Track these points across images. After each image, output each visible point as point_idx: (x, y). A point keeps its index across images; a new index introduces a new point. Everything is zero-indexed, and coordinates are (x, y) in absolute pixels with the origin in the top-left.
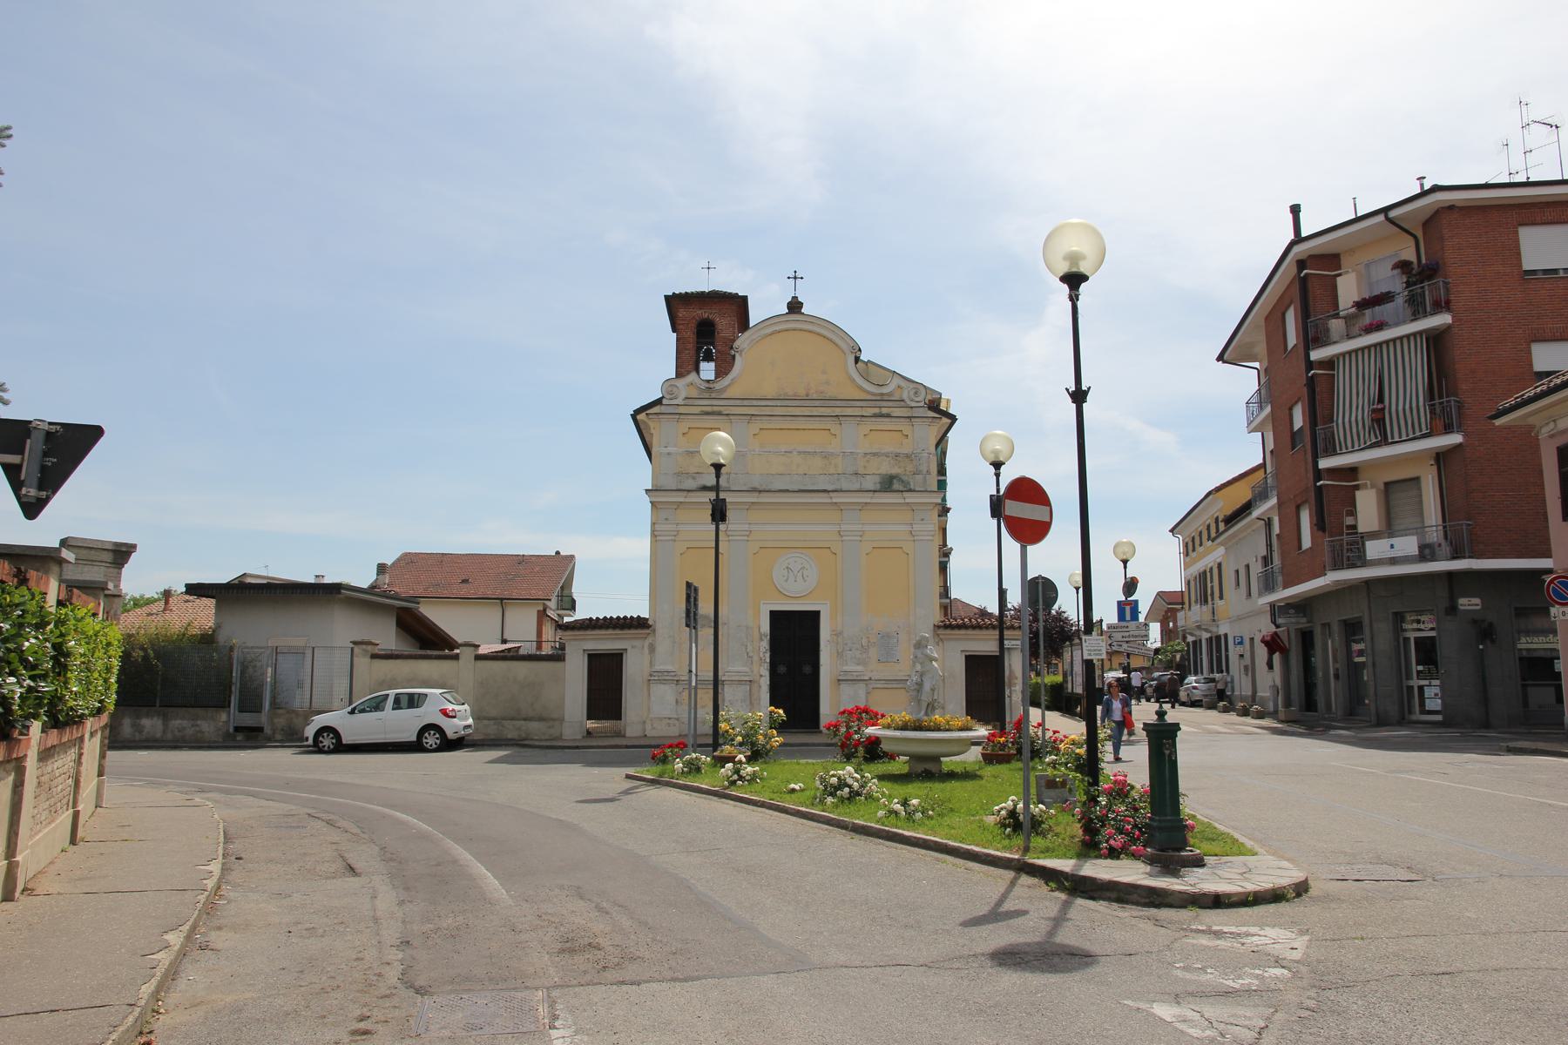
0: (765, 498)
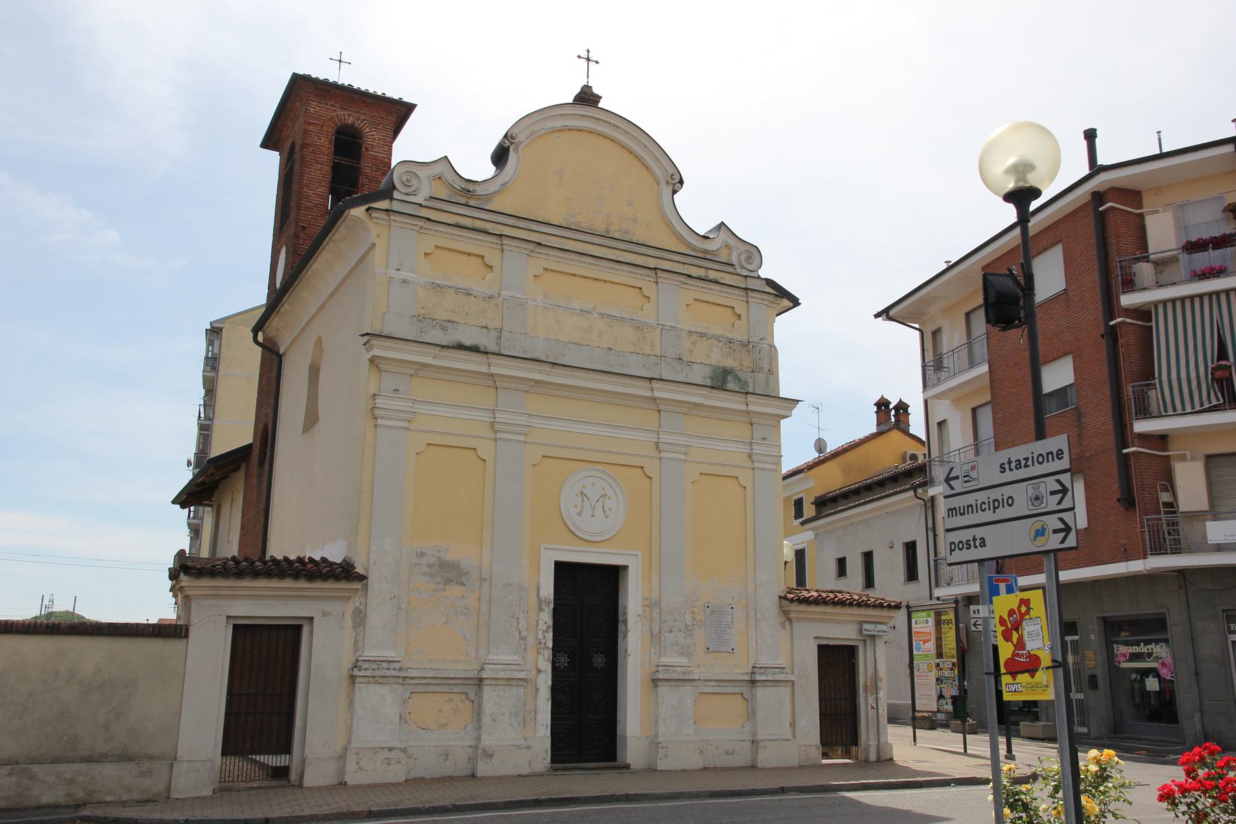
0: (559, 377)
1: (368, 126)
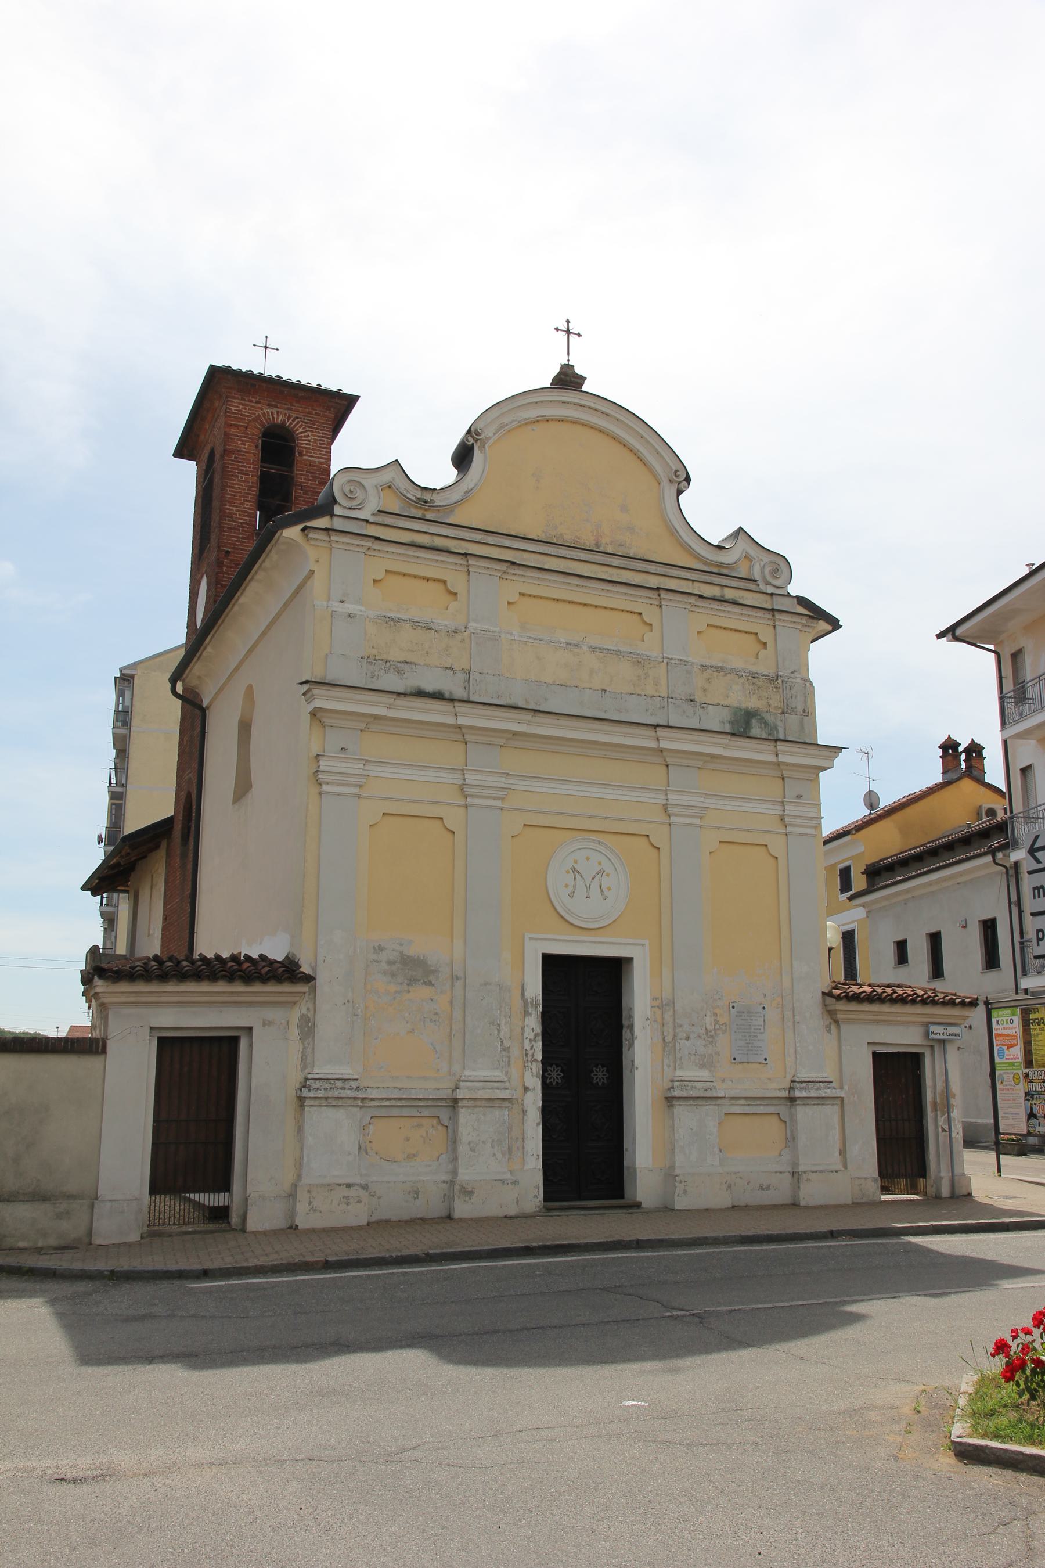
0: (542, 727)
1: (302, 425)
